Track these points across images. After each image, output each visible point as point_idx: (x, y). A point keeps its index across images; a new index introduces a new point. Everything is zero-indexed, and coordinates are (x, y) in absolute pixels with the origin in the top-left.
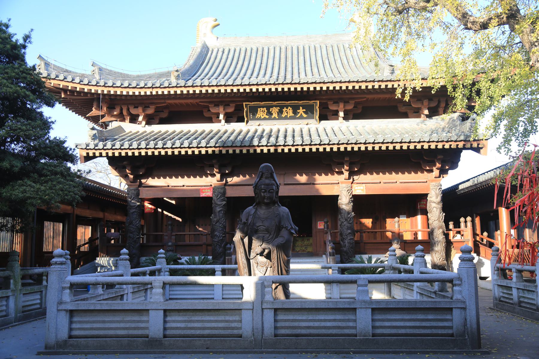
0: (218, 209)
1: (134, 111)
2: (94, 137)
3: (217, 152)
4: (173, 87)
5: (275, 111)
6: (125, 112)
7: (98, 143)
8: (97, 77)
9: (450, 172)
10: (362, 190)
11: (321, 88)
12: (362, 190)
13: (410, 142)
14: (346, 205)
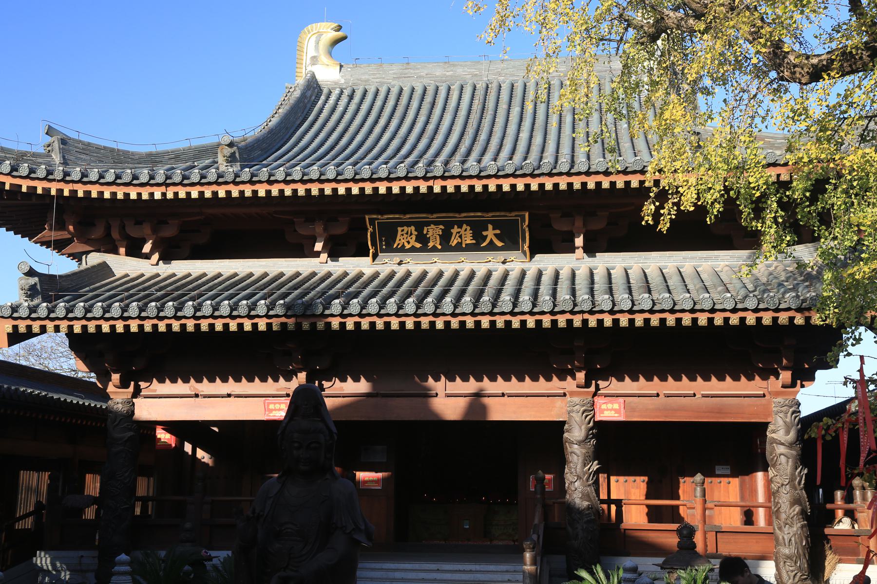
1: (134, 232)
2: (32, 292)
3: (291, 327)
4: (210, 184)
5: (434, 233)
6: (115, 235)
7: (37, 306)
8: (57, 158)
9: (820, 374)
10: (616, 411)
11: (527, 186)
12: (616, 411)
13: (713, 311)
14: (580, 443)
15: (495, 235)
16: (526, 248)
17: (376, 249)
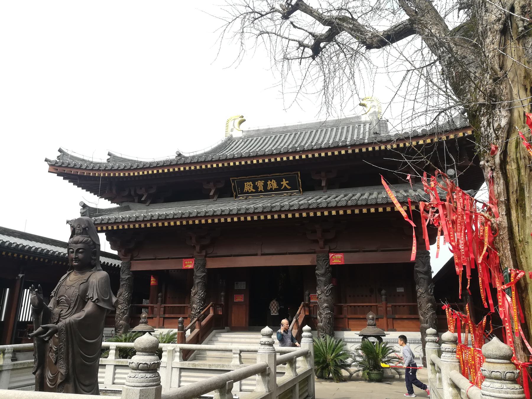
0: (197, 281)
1: (139, 192)
2: (83, 214)
5: (260, 184)
12: (340, 259)
14: (323, 275)
17: (236, 193)
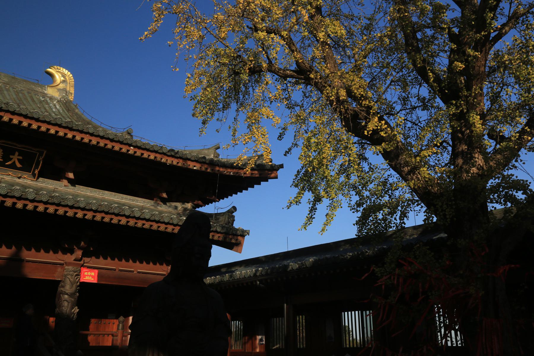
10: (93, 277)
12: (93, 277)
14: (71, 295)
15: (19, 160)
16: (37, 172)
